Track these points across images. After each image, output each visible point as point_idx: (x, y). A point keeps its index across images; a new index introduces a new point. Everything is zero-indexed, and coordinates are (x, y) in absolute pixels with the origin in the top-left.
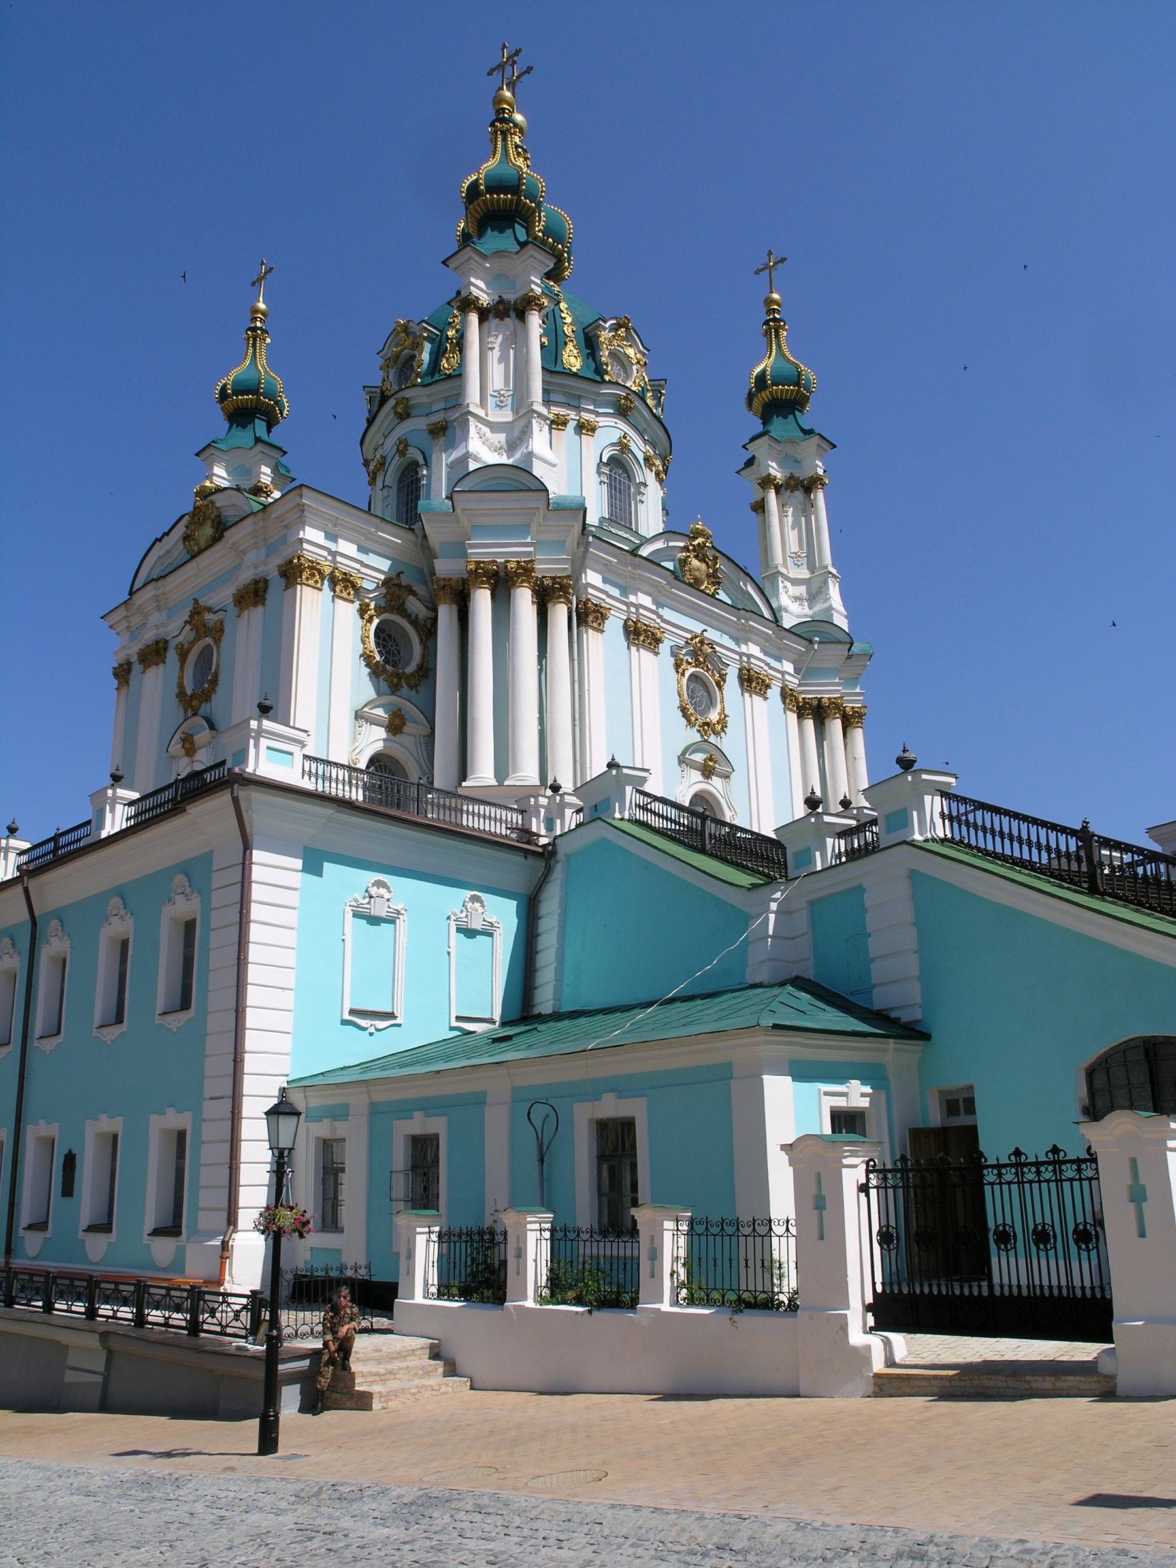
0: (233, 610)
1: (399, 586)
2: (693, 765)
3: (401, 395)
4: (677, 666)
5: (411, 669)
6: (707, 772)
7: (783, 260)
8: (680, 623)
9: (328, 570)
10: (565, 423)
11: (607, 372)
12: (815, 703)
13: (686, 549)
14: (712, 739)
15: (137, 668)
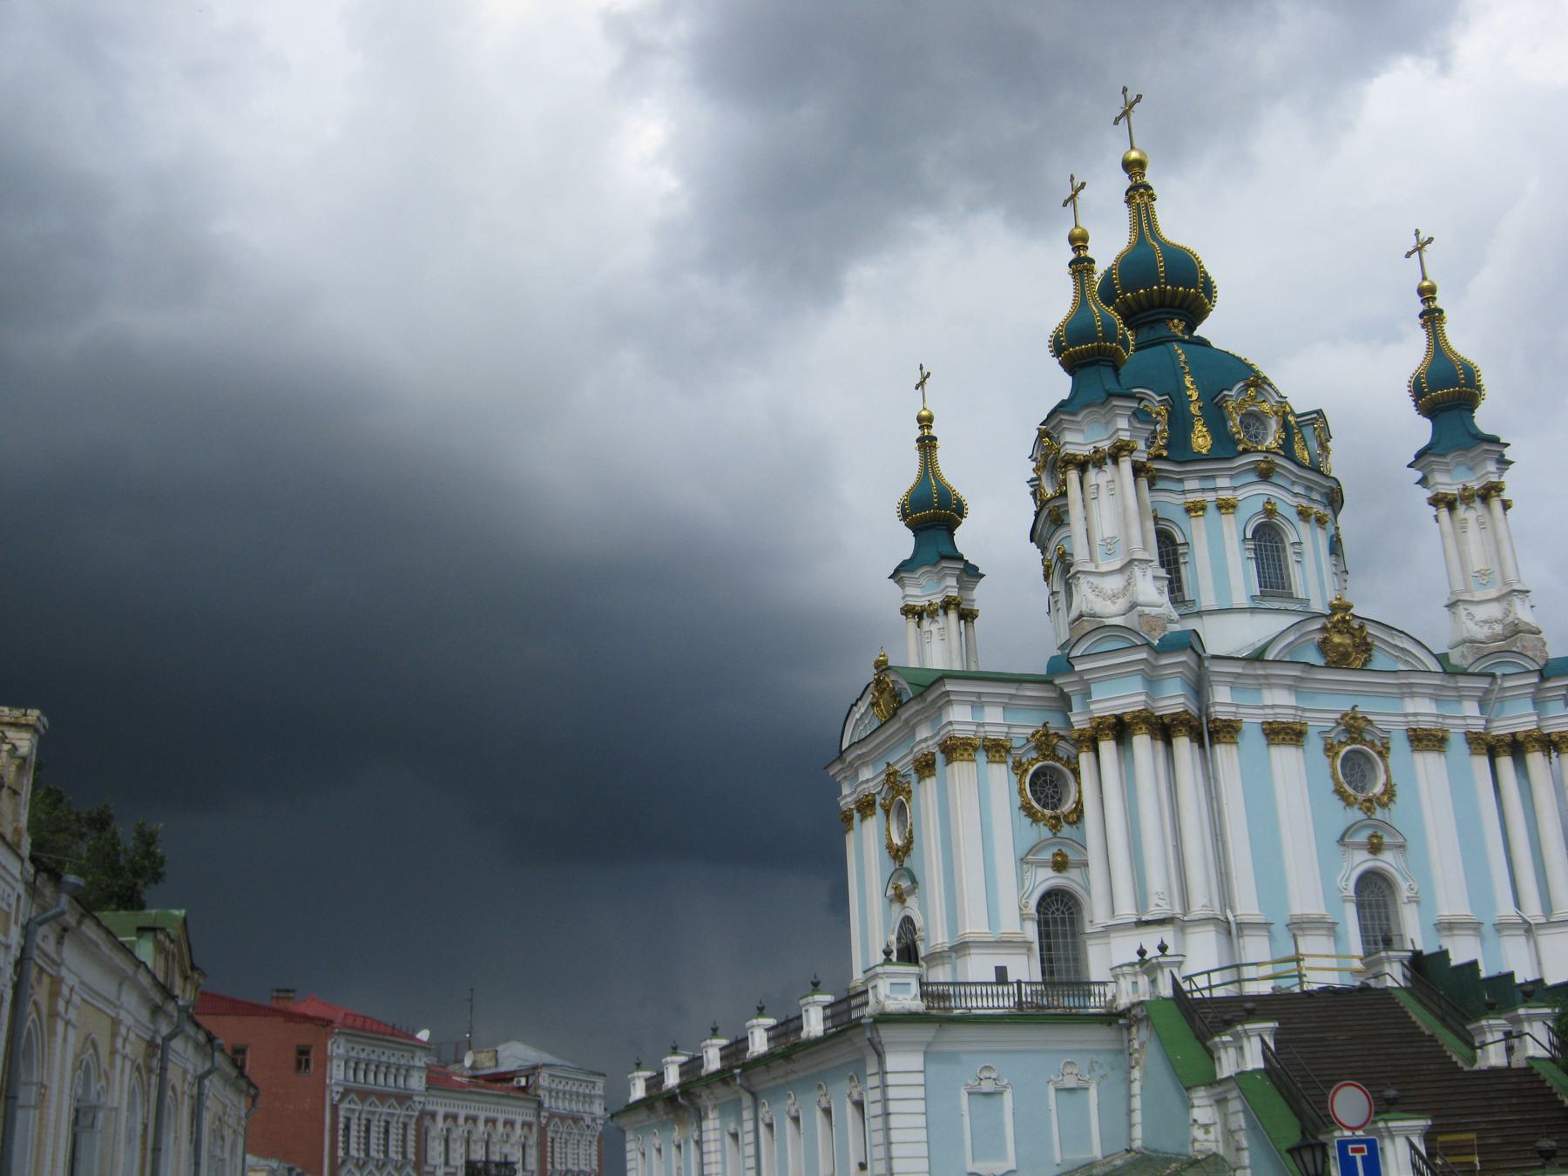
0: (914, 777)
1: (1046, 735)
2: (1358, 846)
3: (1051, 505)
4: (1330, 749)
5: (1068, 806)
6: (1375, 847)
7: (1430, 240)
8: (1323, 710)
9: (978, 742)
10: (1203, 508)
11: (1240, 441)
12: (1509, 739)
13: (1324, 629)
14: (1379, 813)
15: (857, 816)
